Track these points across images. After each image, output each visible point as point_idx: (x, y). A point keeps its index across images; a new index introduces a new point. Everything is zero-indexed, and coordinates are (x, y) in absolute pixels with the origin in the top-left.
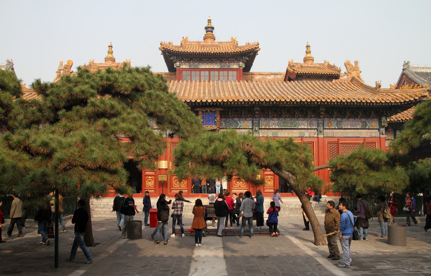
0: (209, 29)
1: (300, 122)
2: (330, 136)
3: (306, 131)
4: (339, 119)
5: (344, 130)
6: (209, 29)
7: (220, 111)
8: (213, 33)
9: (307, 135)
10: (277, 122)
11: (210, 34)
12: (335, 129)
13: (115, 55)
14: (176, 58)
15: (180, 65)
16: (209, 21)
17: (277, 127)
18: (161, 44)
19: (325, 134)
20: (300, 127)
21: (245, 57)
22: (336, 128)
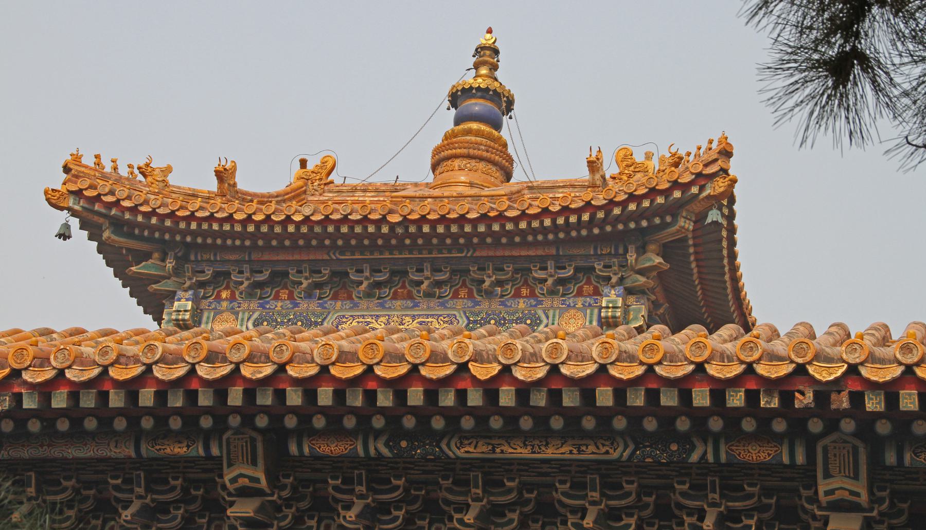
0: (482, 105)
6: (482, 105)
8: (504, 133)
14: (178, 271)
15: (197, 314)
16: (487, 56)
18: (67, 170)
21: (642, 250)
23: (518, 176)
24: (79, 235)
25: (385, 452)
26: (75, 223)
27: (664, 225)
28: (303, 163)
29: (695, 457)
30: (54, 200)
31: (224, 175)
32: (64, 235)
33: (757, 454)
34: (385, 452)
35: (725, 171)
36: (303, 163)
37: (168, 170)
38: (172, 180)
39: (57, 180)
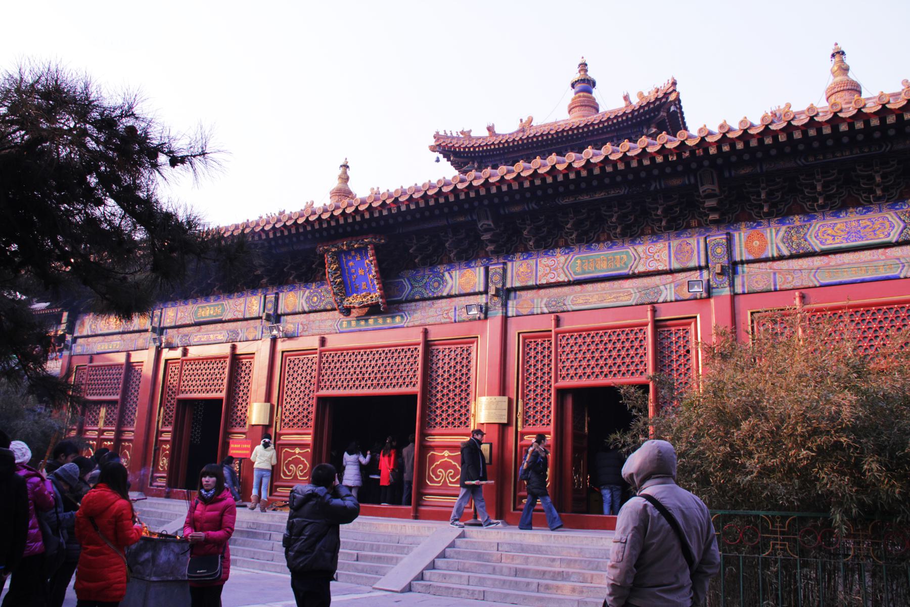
0: (585, 85)
1: (640, 249)
2: (760, 286)
3: (669, 278)
4: (797, 220)
5: (825, 259)
6: (585, 85)
7: (379, 252)
8: (594, 95)
9: (668, 293)
10: (562, 259)
11: (584, 96)
12: (781, 258)
13: (352, 186)
16: (583, 66)
17: (562, 278)
18: (435, 137)
19: (738, 281)
20: (641, 269)
21: (649, 128)
22: (786, 252)
23: (601, 110)
24: (443, 160)
25: (535, 207)
26: (441, 156)
27: (655, 116)
28: (521, 120)
29: (652, 188)
30: (433, 149)
31: (490, 129)
32: (438, 160)
33: (676, 182)
34: (535, 207)
35: (674, 90)
36: (521, 120)
37: (470, 131)
38: (473, 134)
39: (433, 142)
